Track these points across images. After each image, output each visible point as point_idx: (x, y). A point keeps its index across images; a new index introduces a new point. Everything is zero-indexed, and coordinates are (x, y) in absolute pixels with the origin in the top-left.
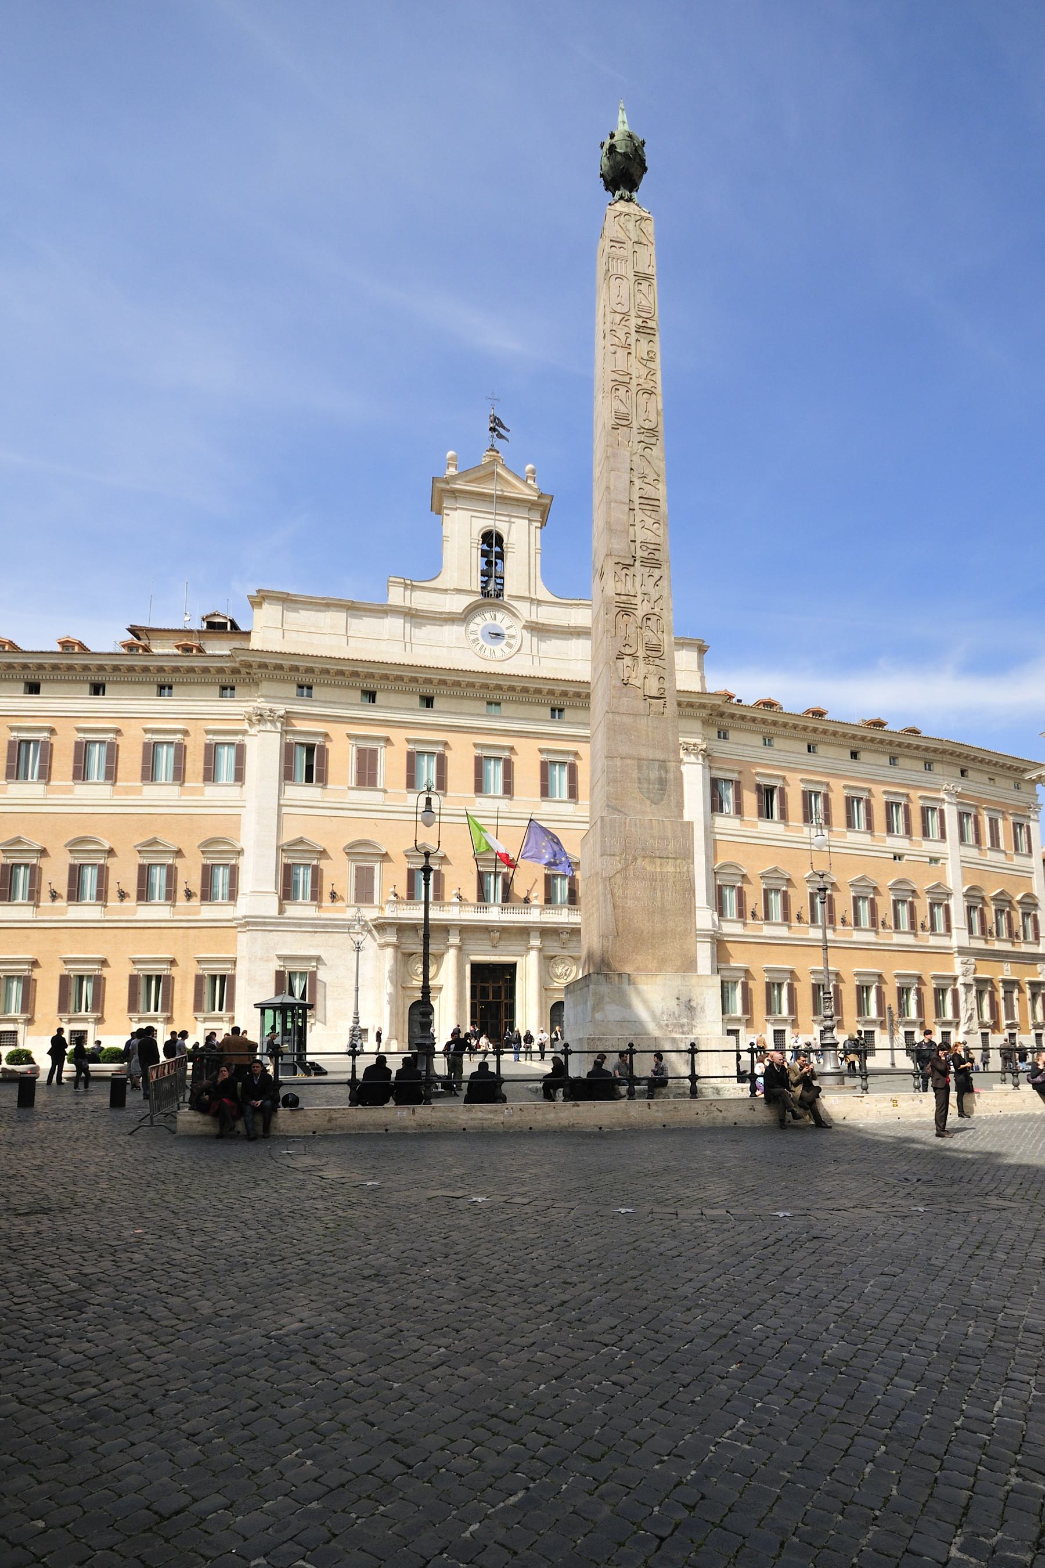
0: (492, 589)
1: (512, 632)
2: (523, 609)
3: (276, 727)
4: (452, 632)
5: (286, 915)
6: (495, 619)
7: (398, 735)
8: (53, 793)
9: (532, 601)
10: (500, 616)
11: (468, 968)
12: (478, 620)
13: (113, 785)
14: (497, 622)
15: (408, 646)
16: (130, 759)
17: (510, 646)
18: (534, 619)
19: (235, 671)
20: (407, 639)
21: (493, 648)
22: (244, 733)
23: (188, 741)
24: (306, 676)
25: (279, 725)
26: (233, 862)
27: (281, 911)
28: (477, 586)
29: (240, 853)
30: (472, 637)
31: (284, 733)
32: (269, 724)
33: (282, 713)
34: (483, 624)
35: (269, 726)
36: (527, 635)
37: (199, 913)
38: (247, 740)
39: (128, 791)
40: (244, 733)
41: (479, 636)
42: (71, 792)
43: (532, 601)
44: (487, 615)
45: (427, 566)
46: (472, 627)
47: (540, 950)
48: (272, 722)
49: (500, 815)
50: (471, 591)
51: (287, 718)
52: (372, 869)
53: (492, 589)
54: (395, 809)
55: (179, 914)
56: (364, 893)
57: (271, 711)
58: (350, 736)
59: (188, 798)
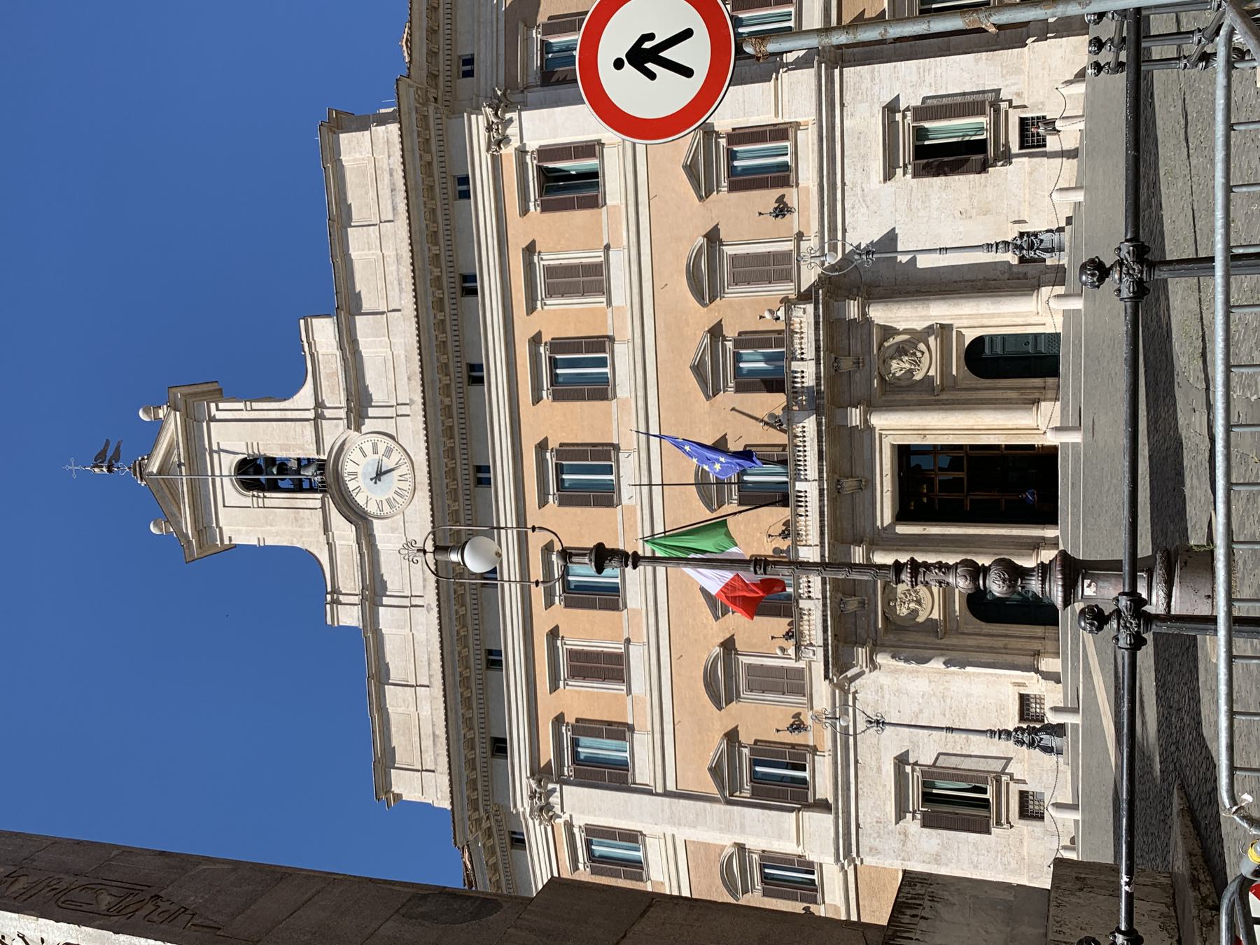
0: (313, 478)
1: (368, 448)
2: (334, 432)
3: (554, 790)
4: (387, 539)
6: (355, 474)
9: (319, 417)
10: (348, 467)
11: (902, 529)
12: (360, 500)
15: (416, 601)
17: (389, 451)
18: (342, 413)
19: (489, 833)
20: (406, 602)
24: (479, 746)
25: (550, 786)
28: (314, 500)
30: (386, 509)
31: (563, 782)
32: (551, 800)
36: (368, 425)
40: (569, 826)
43: (319, 417)
44: (351, 485)
45: (296, 571)
46: (372, 508)
47: (871, 406)
50: (323, 507)
51: (540, 773)
52: (749, 667)
53: (313, 478)
56: (793, 683)
57: (532, 797)
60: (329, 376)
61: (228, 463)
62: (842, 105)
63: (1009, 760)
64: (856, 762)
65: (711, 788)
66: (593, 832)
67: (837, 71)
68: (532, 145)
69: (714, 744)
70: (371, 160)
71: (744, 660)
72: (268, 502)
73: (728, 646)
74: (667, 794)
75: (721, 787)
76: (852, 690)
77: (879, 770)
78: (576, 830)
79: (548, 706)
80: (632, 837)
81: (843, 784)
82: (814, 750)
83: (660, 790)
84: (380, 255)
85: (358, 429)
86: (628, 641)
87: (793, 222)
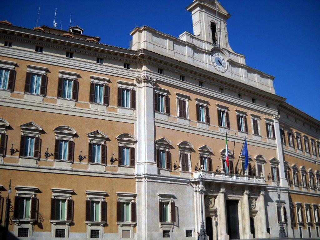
5: (161, 174)
7: (193, 97)
8: (47, 102)
10: (220, 55)
13: (76, 101)
14: (220, 57)
16: (84, 91)
21: (219, 67)
22: (135, 85)
23: (110, 85)
26: (132, 146)
27: (159, 173)
29: (136, 142)
30: (213, 61)
33: (155, 80)
34: (216, 57)
35: (150, 85)
37: (53, 165)
38: (136, 89)
39: (82, 105)
40: (135, 85)
41: (215, 61)
42: (56, 102)
44: (216, 54)
48: (151, 83)
49: (236, 138)
54: (213, 133)
55: (108, 170)
58: (177, 94)
59: (111, 113)
60: (238, 59)
61: (216, 21)
62: (284, 192)
63: (178, 227)
64: (172, 184)
65: (159, 138)
66: (133, 93)
67: (287, 192)
68: (274, 124)
69: (170, 142)
70: (267, 86)
71: (189, 154)
72: (210, 28)
73: (192, 150)
74: (155, 122)
75: (159, 141)
76: (188, 184)
77: (170, 190)
78: (132, 87)
79: (174, 91)
80: (133, 106)
81: (165, 179)
82: (170, 171)
83: (156, 120)
84: (255, 81)
85: (228, 61)
86: (190, 121)
87: (267, 180)
